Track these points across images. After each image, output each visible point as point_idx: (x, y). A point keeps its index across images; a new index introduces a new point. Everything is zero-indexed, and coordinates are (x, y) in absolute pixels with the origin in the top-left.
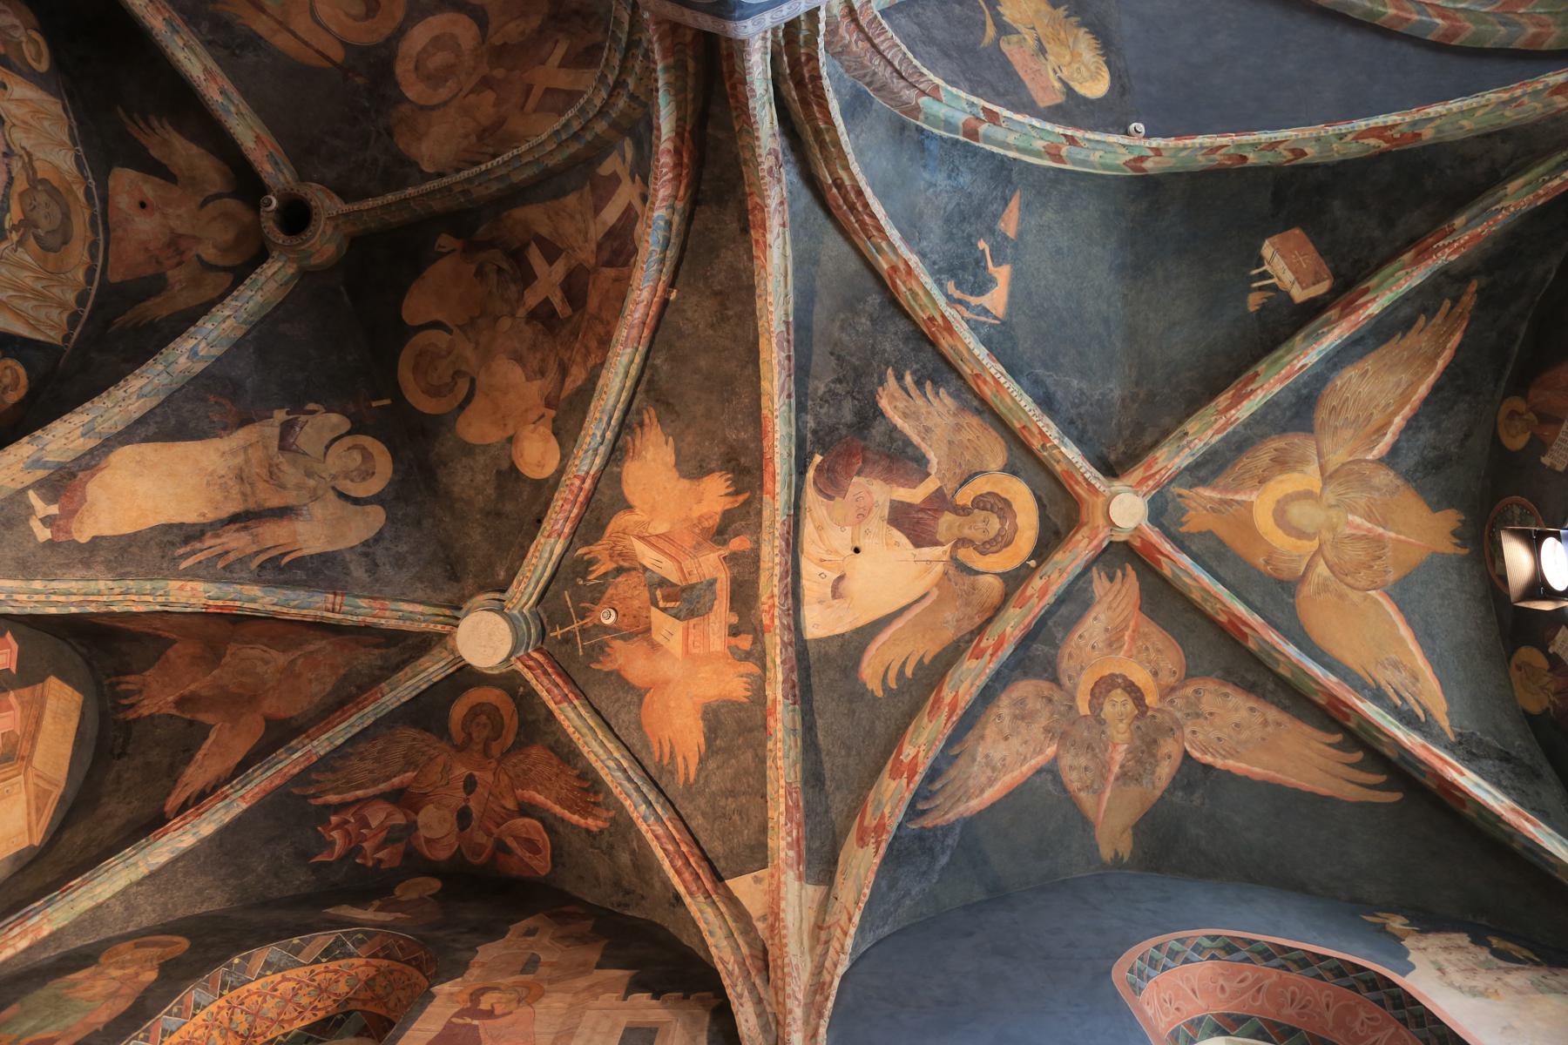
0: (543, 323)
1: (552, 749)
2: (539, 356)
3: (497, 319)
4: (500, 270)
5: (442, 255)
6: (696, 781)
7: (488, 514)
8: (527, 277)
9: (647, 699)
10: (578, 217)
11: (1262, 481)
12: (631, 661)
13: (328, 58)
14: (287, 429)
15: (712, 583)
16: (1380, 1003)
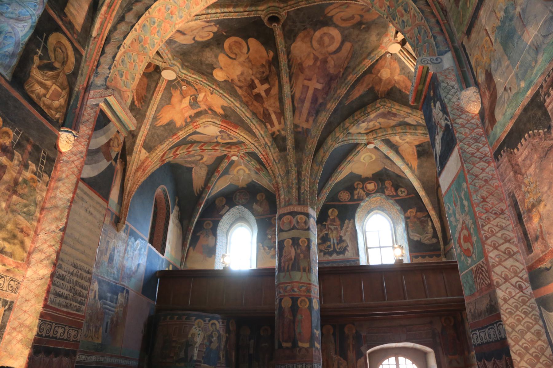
0: (251, 84)
1: (148, 84)
2: (243, 81)
3: (252, 69)
4: (263, 73)
5: (267, 53)
6: (157, 127)
7: (201, 61)
8: (262, 84)
9: (169, 105)
10: (274, 105)
11: (246, 167)
12: (176, 95)
13: (327, 14)
14: (210, 26)
15: (200, 107)
16: (166, 214)
